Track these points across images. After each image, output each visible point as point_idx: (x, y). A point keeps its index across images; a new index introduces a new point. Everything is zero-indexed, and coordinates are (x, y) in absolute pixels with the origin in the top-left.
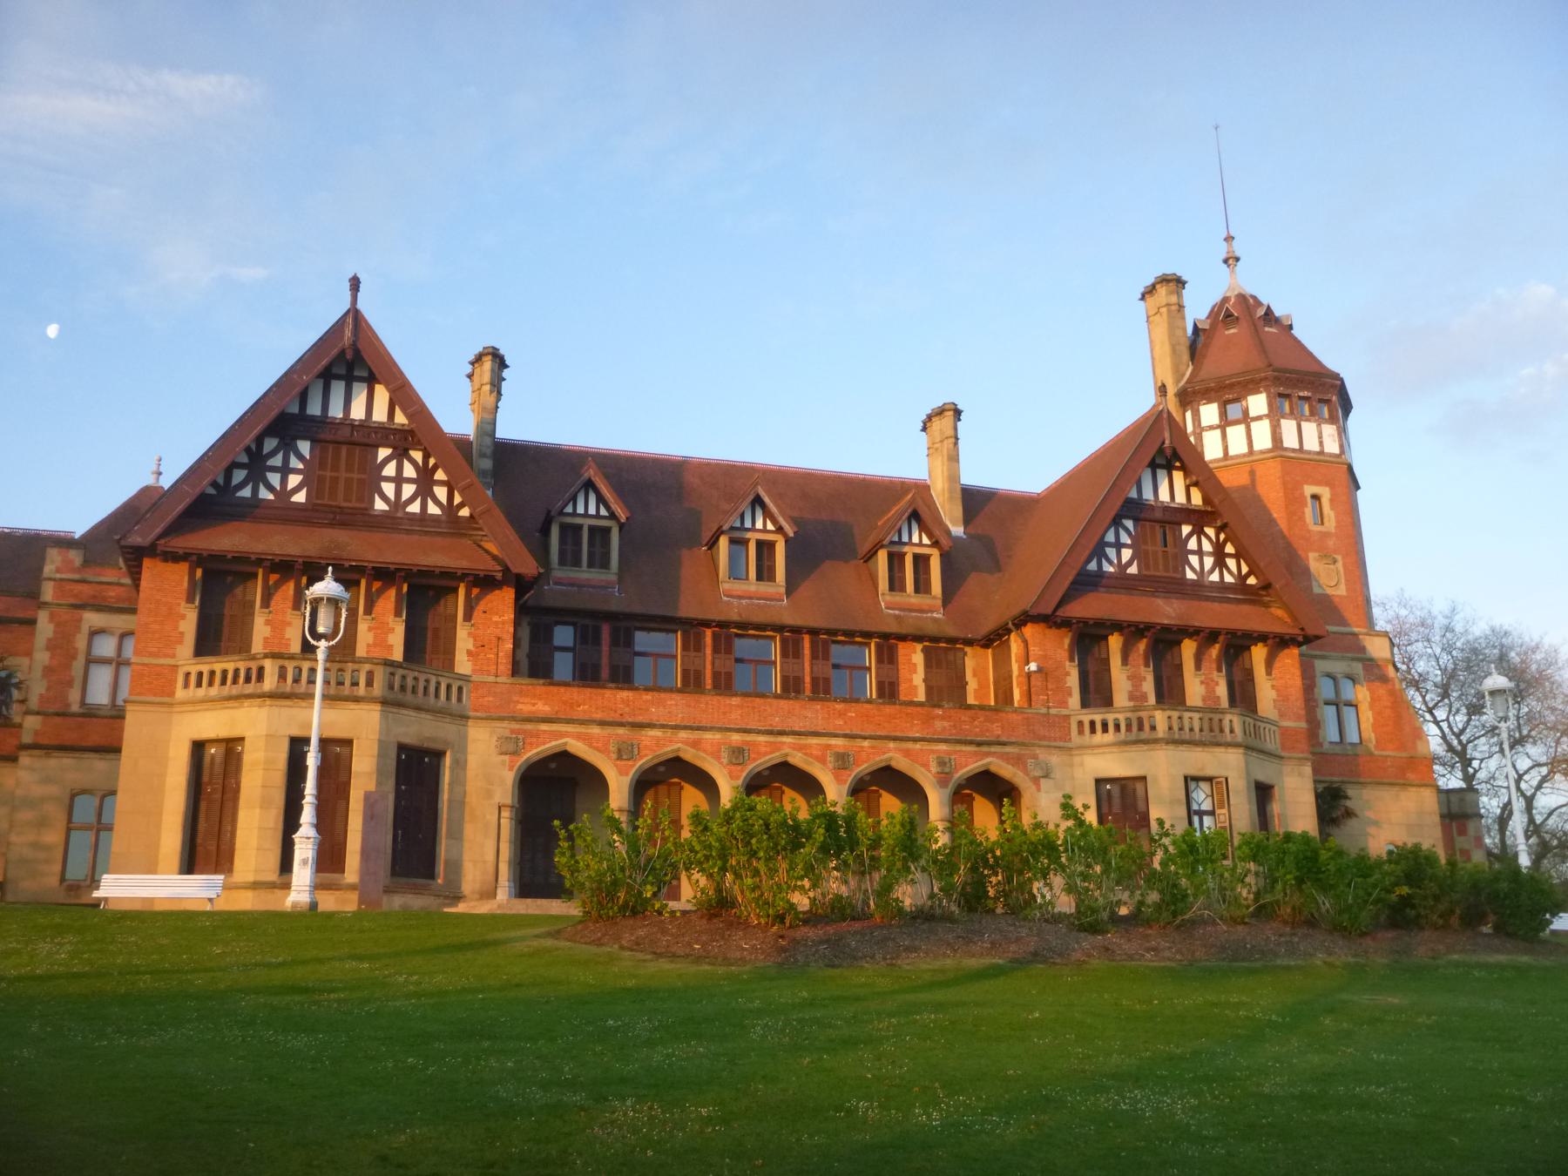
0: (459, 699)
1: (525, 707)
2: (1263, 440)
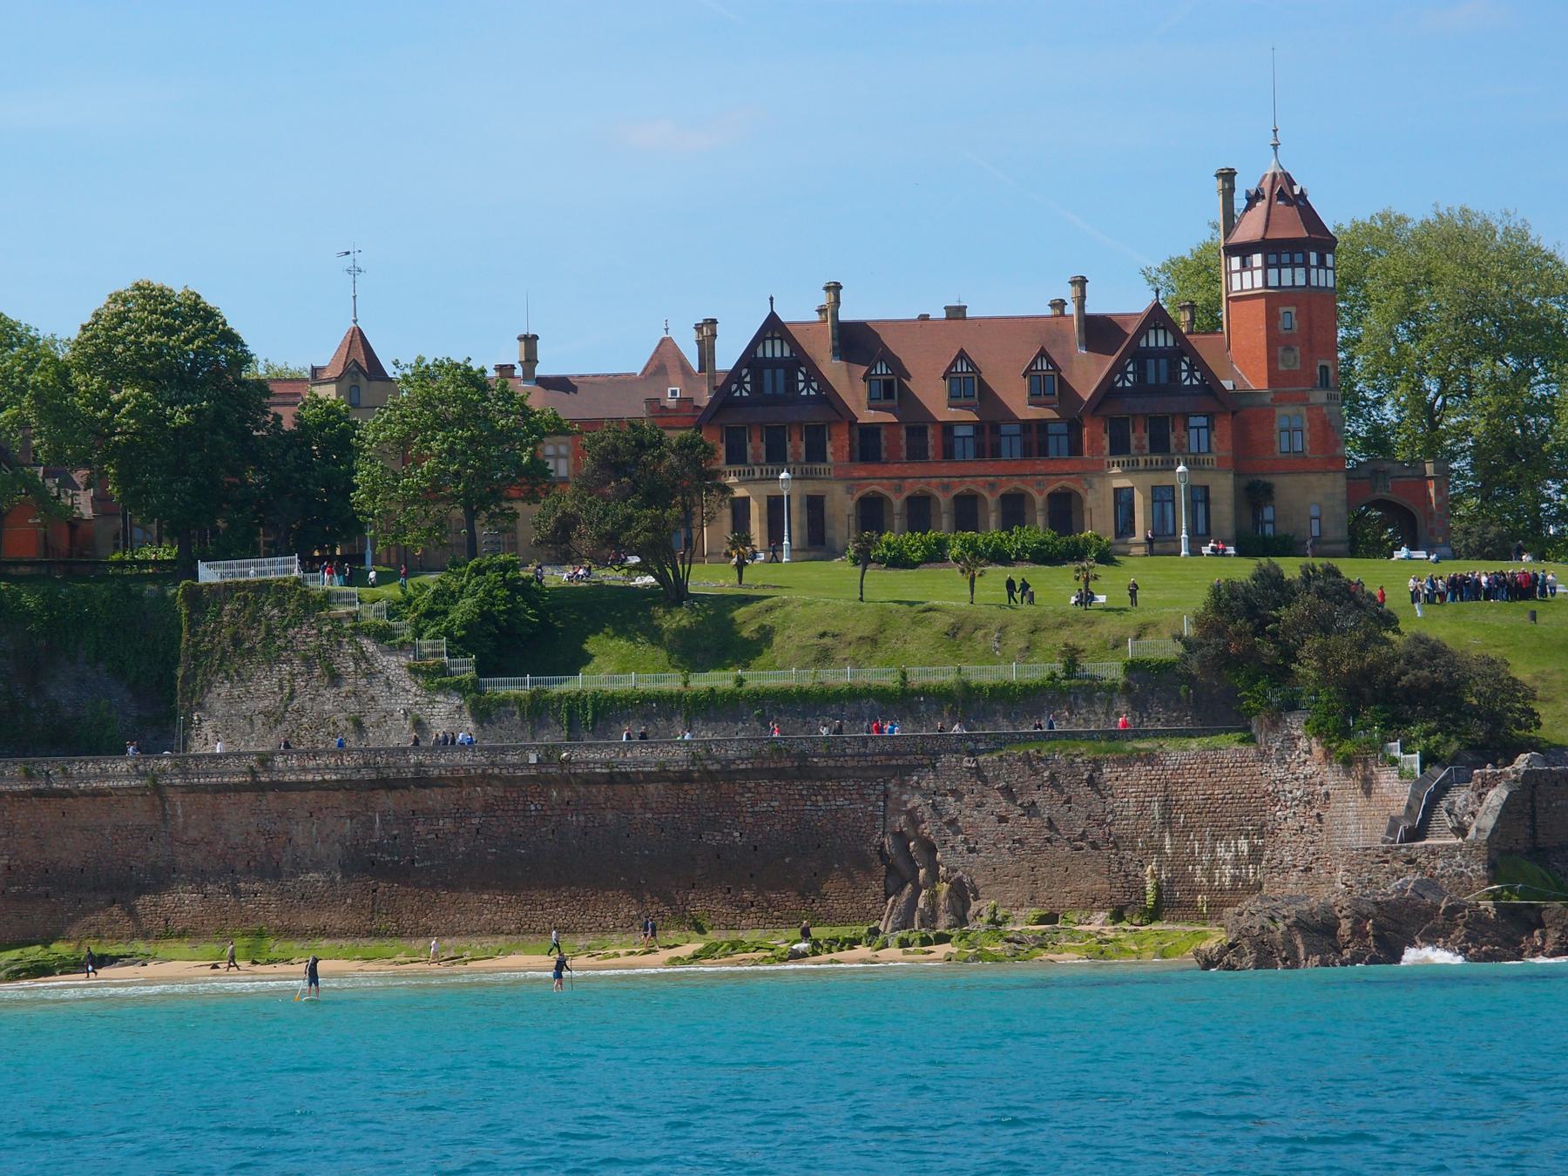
1: (856, 474)
2: (1259, 283)
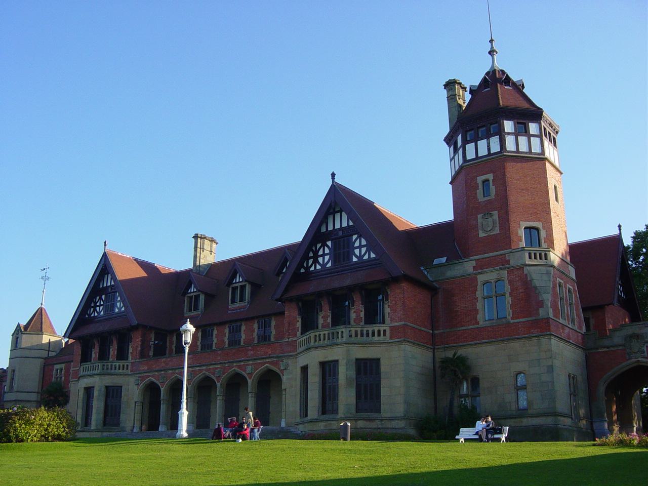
0: (127, 369)
2: (461, 162)
